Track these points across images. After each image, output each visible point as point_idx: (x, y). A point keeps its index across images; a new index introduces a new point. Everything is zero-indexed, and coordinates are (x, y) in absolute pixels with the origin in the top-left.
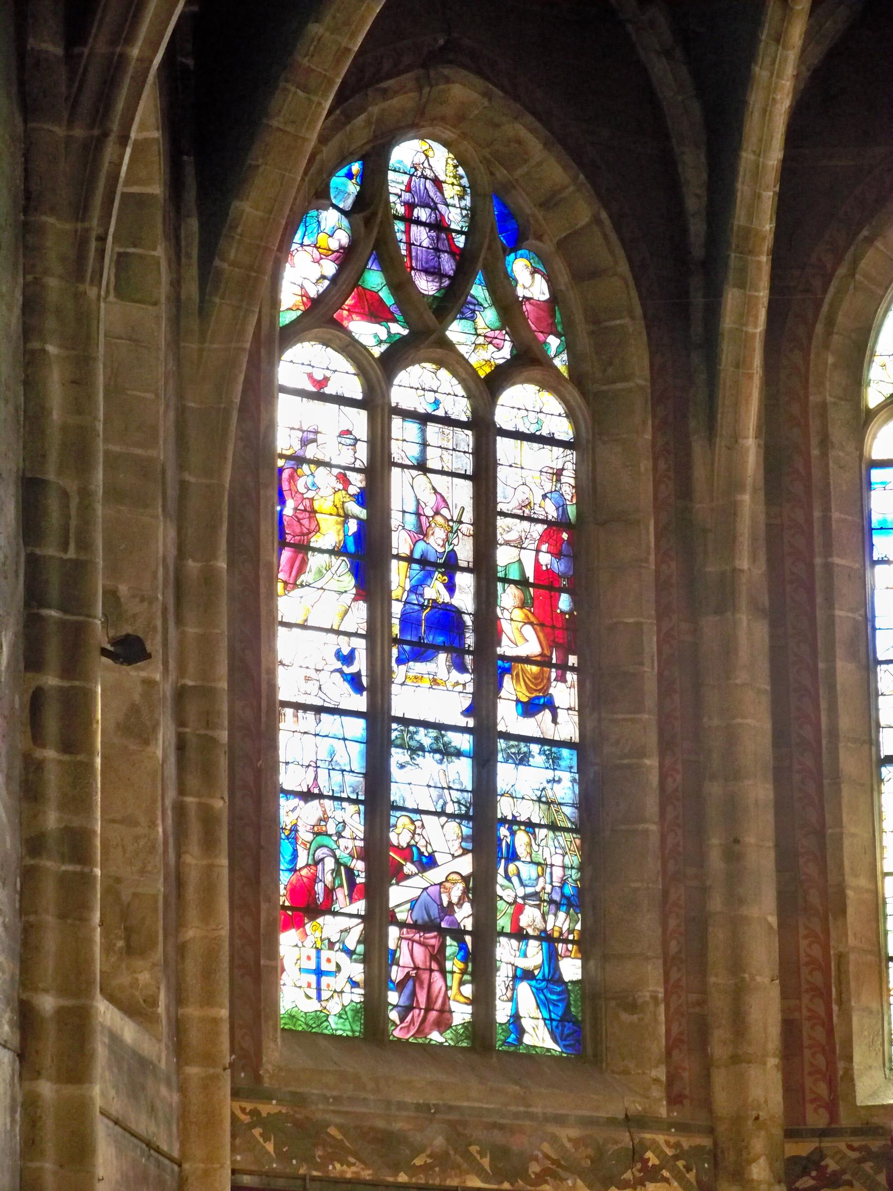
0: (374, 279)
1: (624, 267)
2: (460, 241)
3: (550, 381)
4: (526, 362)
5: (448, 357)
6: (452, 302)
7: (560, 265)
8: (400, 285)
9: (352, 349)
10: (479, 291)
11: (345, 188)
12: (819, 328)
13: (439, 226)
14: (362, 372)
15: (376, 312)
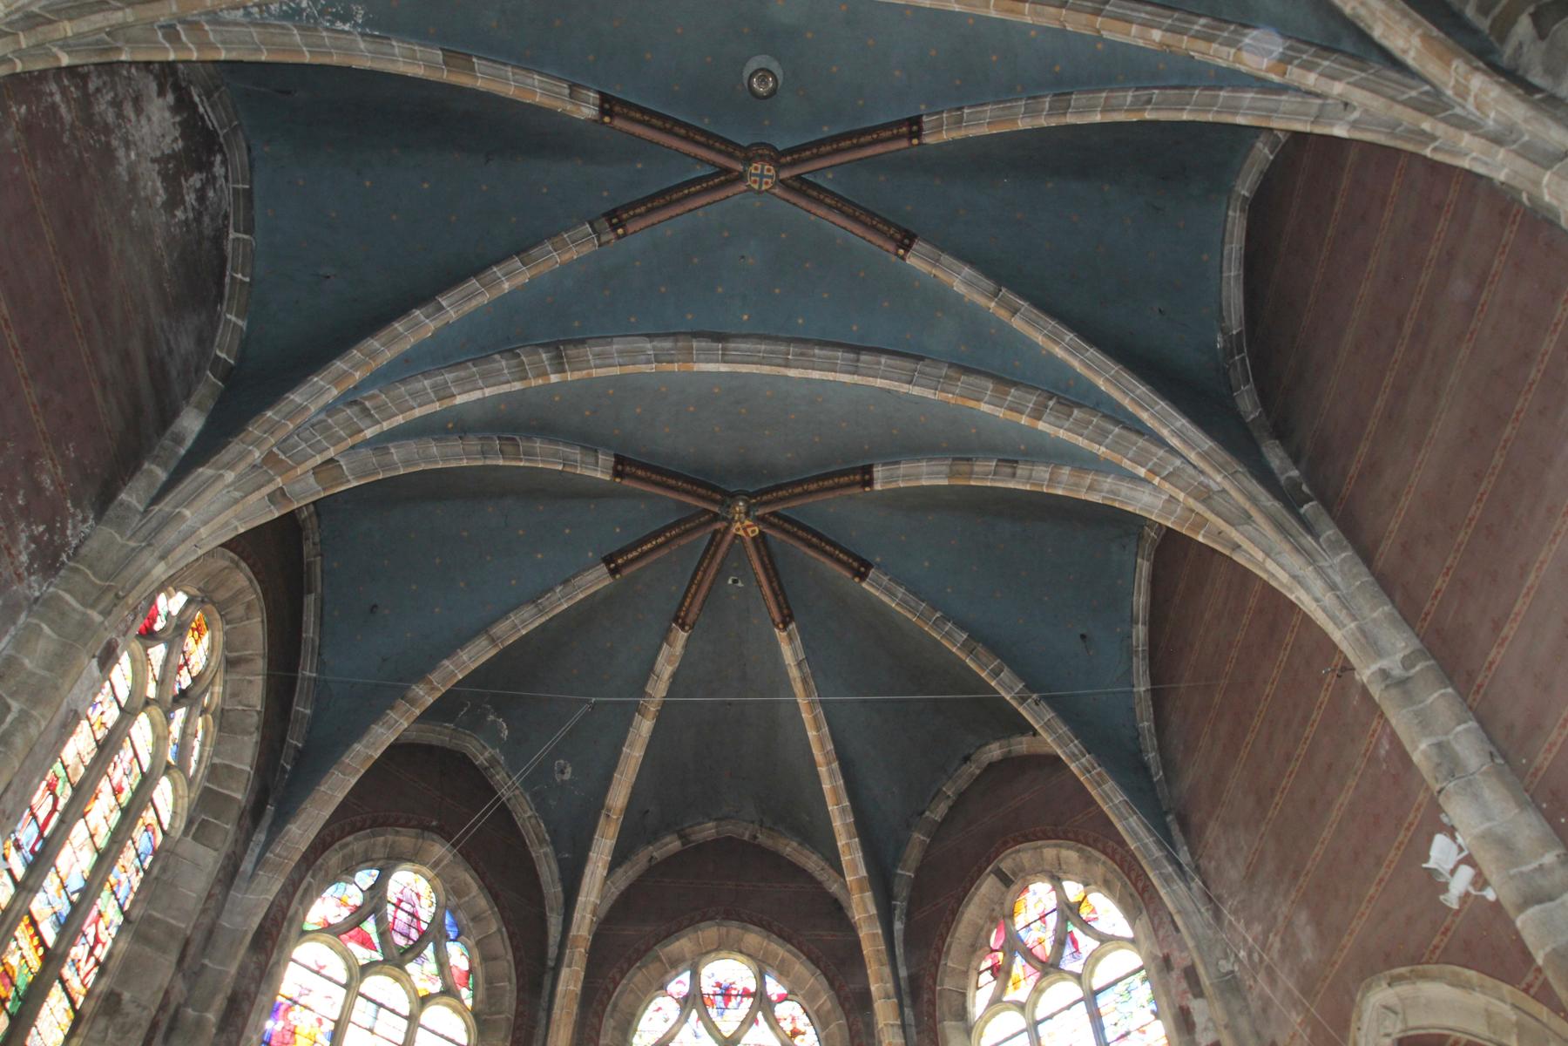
0: (370, 926)
1: (510, 957)
2: (424, 926)
3: (459, 1010)
4: (449, 991)
5: (403, 979)
6: (414, 951)
7: (476, 952)
8: (384, 934)
9: (347, 957)
10: (429, 951)
11: (366, 878)
12: (609, 1008)
13: (413, 915)
14: (349, 969)
15: (366, 942)
